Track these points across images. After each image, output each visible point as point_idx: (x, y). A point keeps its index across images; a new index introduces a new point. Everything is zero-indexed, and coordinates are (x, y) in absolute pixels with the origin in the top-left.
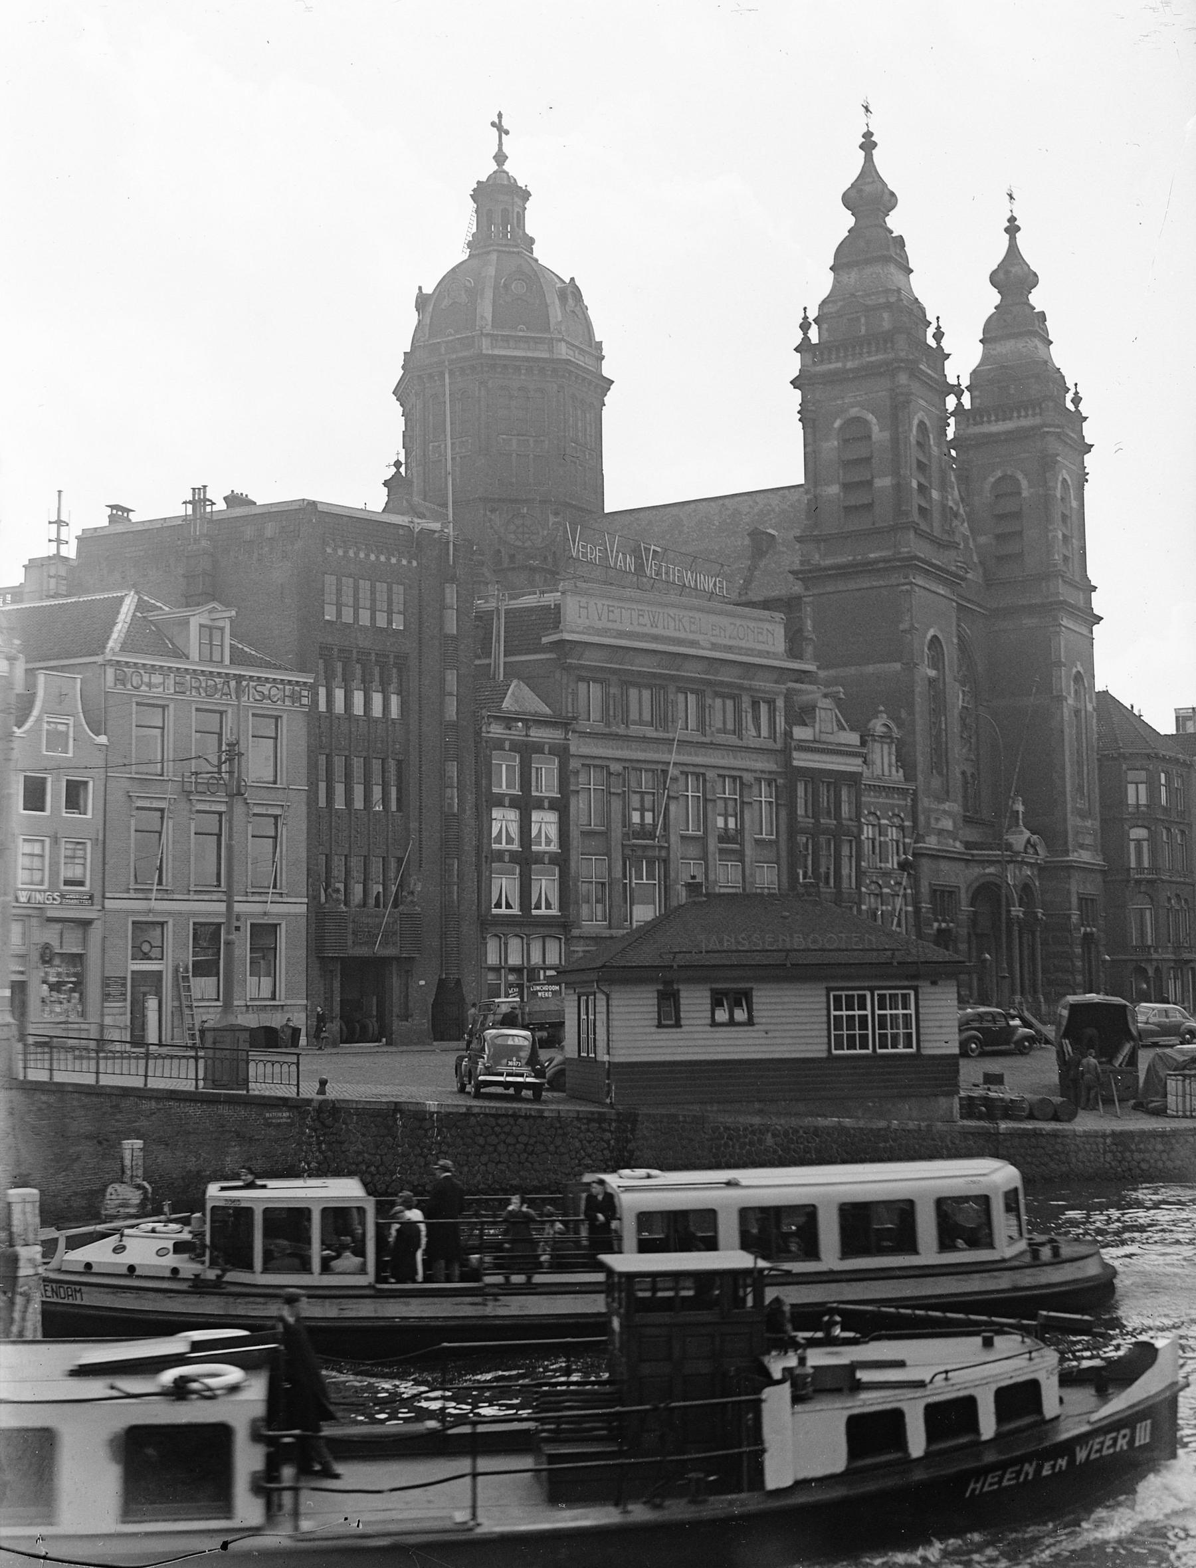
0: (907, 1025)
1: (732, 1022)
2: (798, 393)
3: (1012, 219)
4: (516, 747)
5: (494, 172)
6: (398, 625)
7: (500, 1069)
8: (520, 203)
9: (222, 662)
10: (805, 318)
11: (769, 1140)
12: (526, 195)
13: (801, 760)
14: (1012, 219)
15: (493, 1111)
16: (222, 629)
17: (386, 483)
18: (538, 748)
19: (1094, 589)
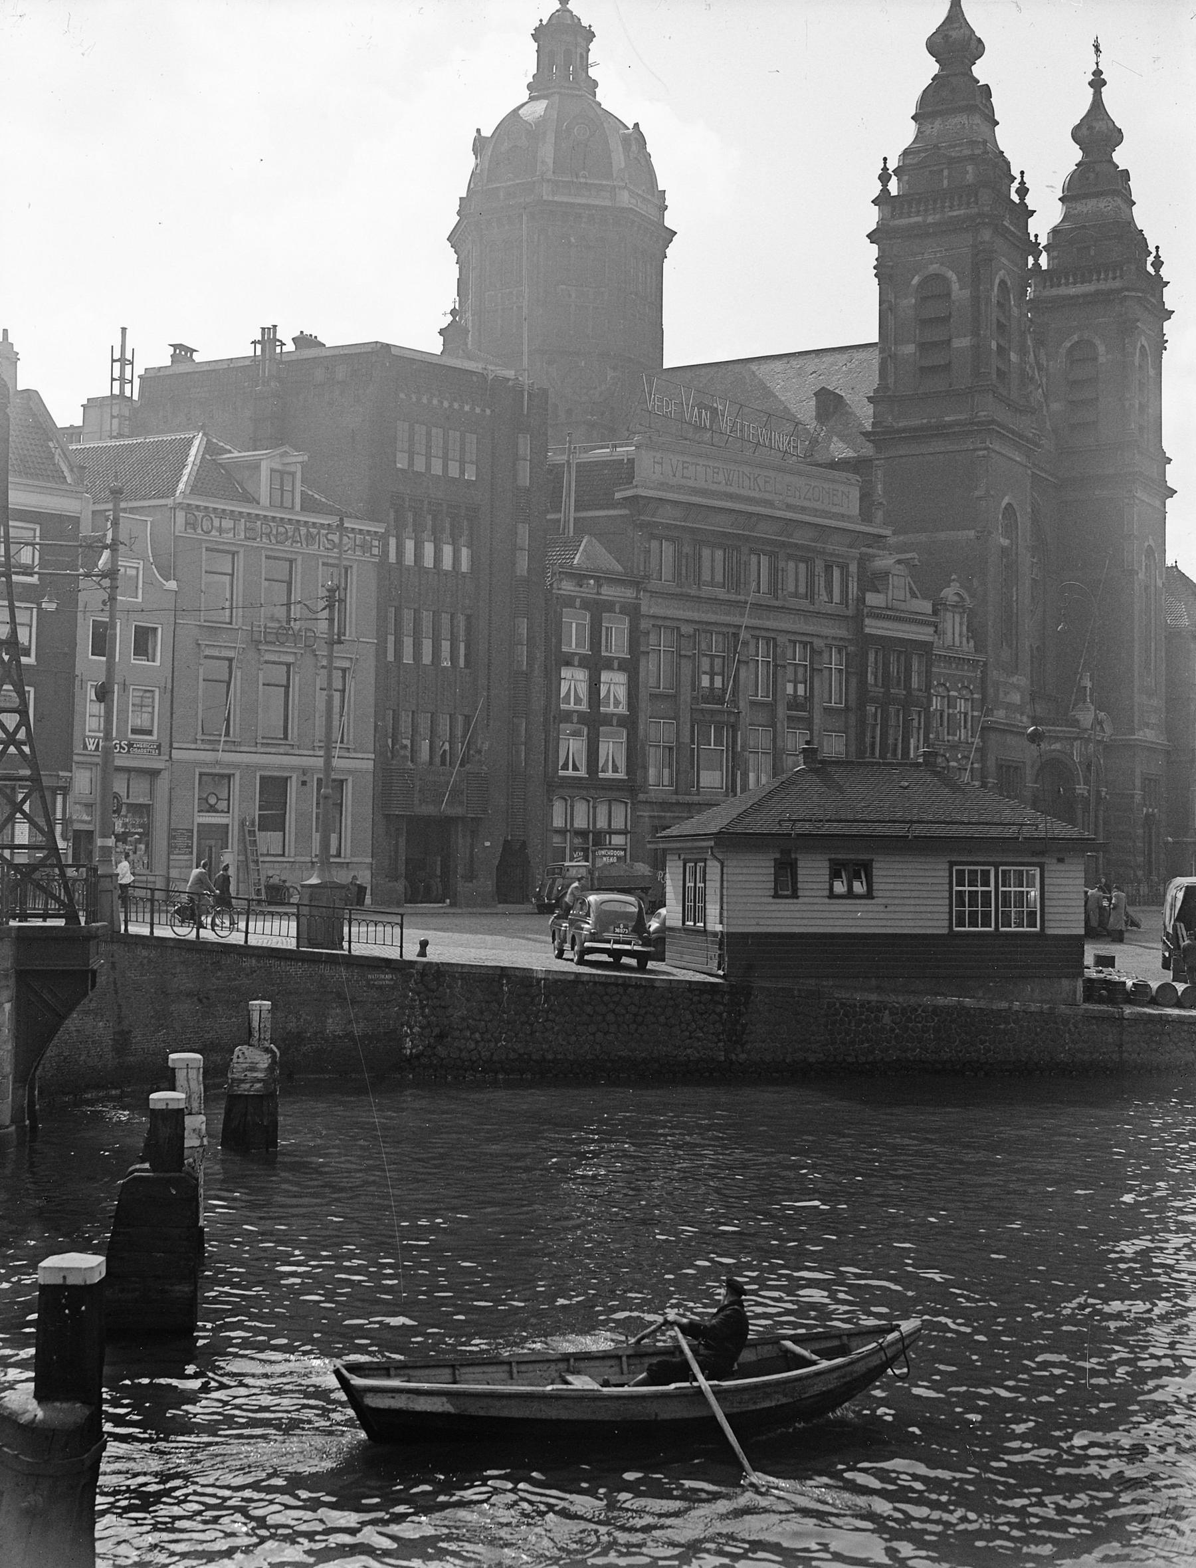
0: (987, 903)
1: (850, 894)
2: (875, 246)
3: (1098, 73)
4: (586, 605)
5: (557, 11)
6: (471, 475)
7: (606, 935)
8: (584, 44)
9: (293, 508)
10: (885, 169)
11: (887, 1018)
12: (590, 35)
13: (873, 627)
14: (1098, 73)
15: (603, 979)
16: (293, 474)
17: (441, 332)
18: (609, 606)
19: (1169, 461)
